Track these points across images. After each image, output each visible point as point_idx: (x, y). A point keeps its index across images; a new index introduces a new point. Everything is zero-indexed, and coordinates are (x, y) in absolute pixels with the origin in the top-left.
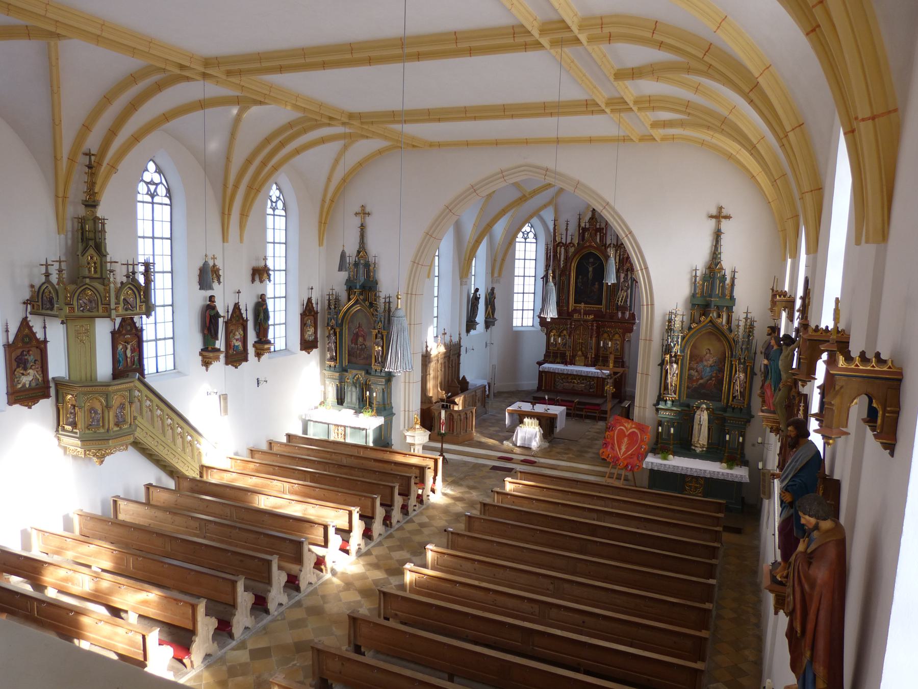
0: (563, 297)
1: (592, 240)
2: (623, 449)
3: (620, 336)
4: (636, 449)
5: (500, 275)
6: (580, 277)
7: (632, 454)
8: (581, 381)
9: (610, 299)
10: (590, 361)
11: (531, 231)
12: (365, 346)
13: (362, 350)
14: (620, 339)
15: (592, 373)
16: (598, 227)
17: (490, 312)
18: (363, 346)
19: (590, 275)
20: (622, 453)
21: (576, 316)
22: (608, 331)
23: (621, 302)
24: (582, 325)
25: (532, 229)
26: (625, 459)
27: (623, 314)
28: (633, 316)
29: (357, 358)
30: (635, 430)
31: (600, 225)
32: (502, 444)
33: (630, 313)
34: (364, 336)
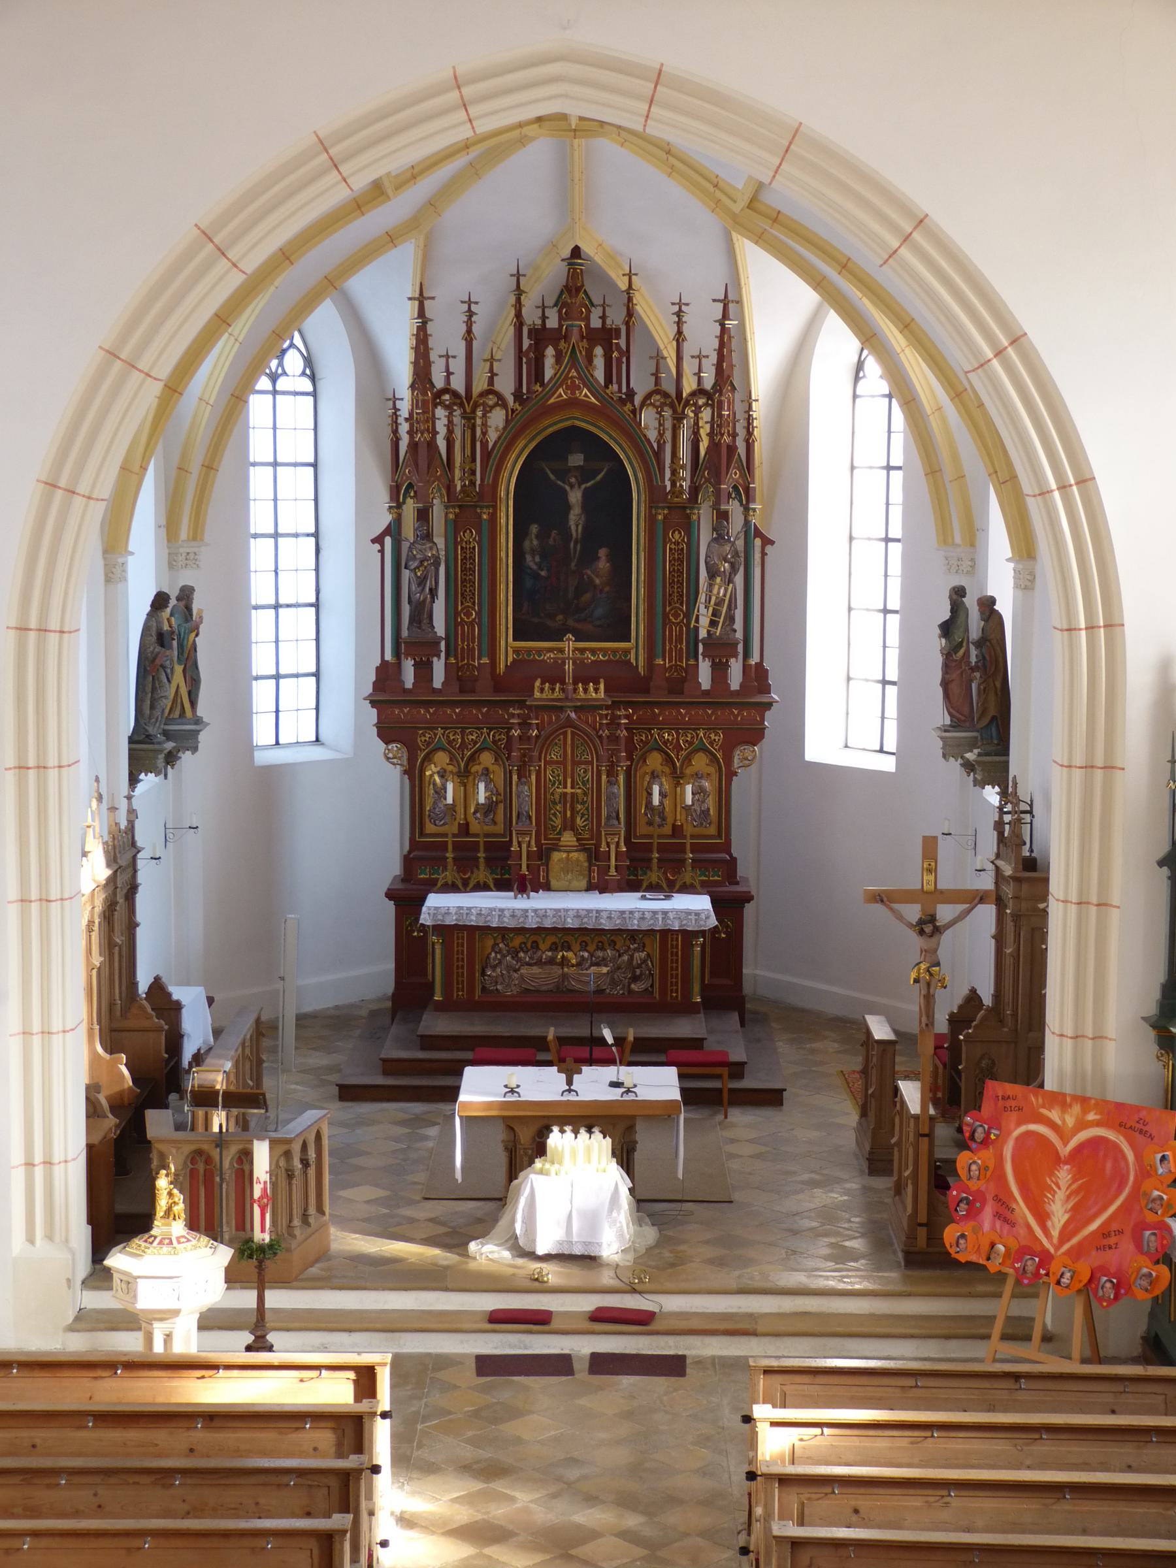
0: (468, 615)
1: (580, 378)
2: (1059, 1214)
3: (714, 759)
4: (1126, 1208)
5: (197, 534)
6: (534, 529)
7: (1104, 1233)
8: (592, 955)
9: (665, 616)
10: (613, 872)
14: (712, 770)
15: (643, 918)
16: (596, 323)
17: (184, 691)
19: (575, 519)
20: (1055, 1233)
21: (541, 693)
22: (666, 743)
23: (713, 623)
24: (569, 723)
26: (1077, 1253)
27: (720, 670)
28: (758, 678)
30: (1111, 1135)
31: (603, 318)
32: (465, 1254)
33: (746, 667)
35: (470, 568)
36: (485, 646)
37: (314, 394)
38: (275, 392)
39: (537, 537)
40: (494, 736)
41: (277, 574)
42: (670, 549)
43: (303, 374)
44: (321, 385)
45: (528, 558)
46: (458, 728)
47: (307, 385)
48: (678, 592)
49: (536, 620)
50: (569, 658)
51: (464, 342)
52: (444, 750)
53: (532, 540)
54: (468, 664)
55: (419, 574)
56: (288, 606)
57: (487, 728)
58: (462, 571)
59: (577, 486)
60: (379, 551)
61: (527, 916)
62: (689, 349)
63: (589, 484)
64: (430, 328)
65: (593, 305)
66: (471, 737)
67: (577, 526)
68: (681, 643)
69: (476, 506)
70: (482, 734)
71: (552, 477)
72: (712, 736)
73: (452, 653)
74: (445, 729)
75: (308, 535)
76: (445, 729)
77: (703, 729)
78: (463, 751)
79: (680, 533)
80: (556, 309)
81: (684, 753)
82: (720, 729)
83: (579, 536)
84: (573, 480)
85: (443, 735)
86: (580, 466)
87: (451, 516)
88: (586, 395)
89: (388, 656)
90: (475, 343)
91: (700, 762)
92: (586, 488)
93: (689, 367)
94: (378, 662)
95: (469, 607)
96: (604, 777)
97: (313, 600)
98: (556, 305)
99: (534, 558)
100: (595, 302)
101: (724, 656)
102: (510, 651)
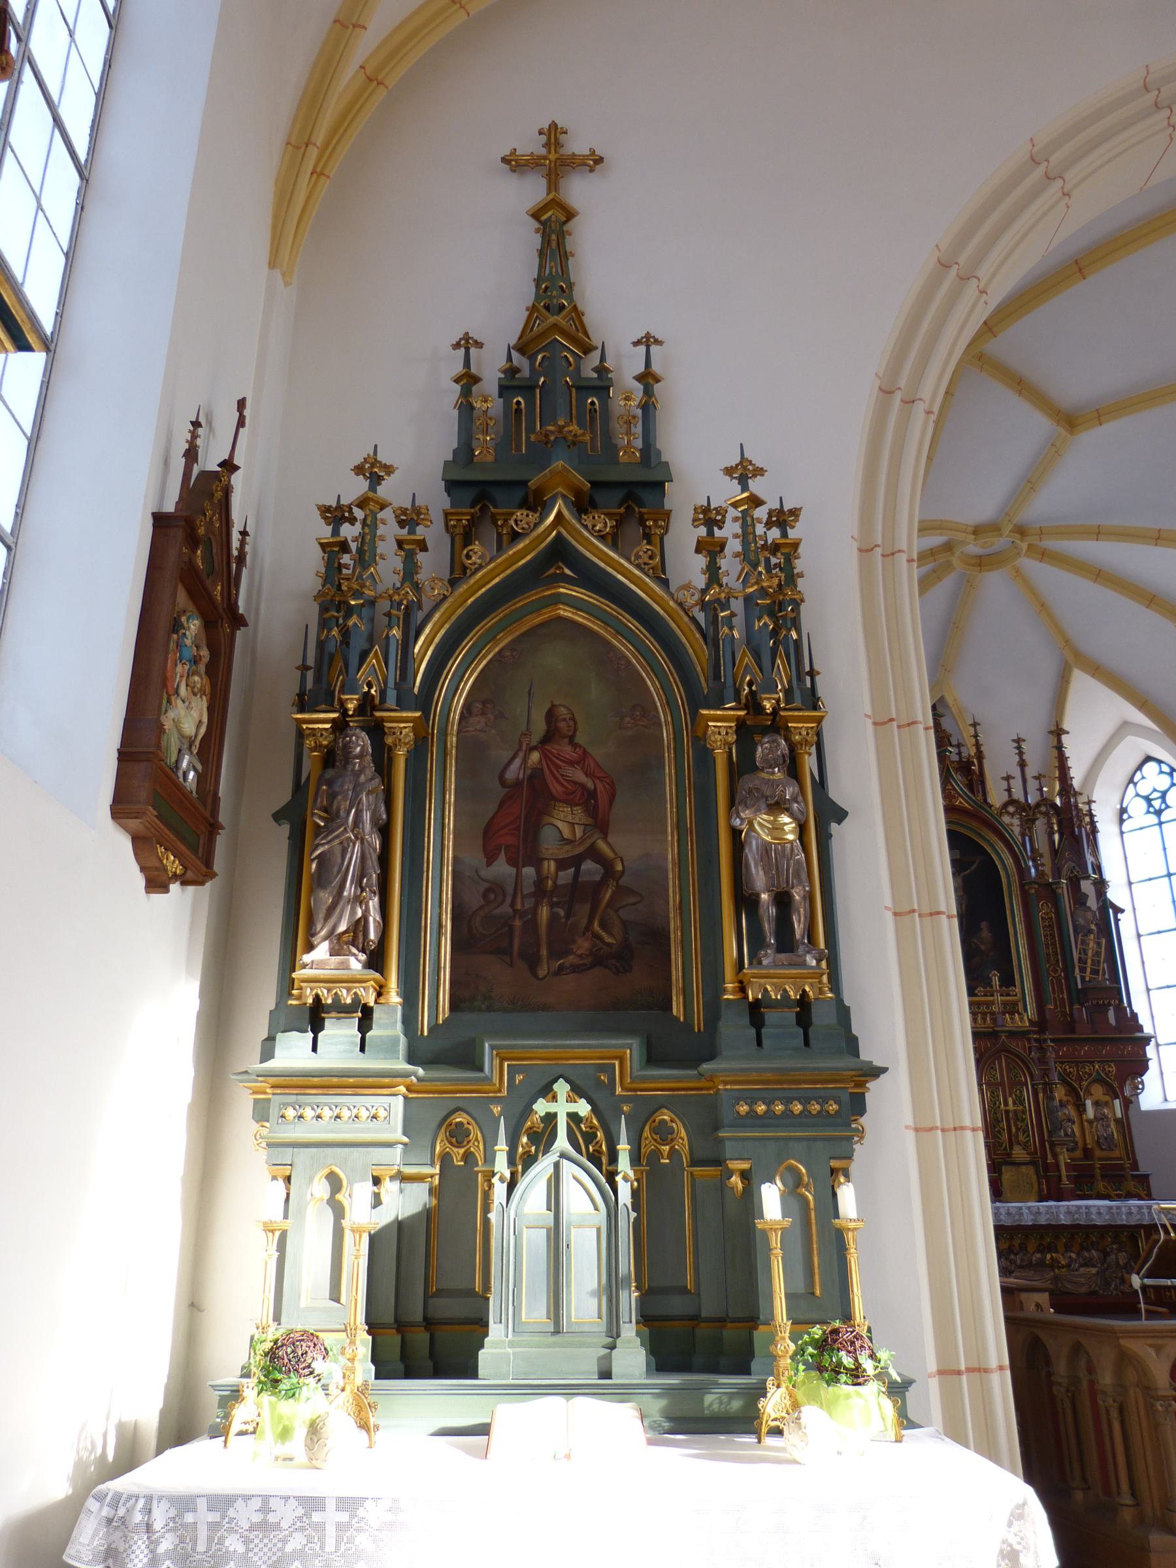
12: (607, 864)
13: (577, 892)
15: (1130, 1213)
18: (588, 865)
29: (533, 963)
34: (593, 794)
42: (1042, 918)
48: (1053, 952)
61: (1022, 1214)
62: (1031, 772)
63: (966, 872)
68: (1063, 994)
72: (1106, 1067)
77: (1098, 1062)
79: (1047, 905)
81: (1085, 1084)
82: (1111, 1061)
88: (960, 803)
91: (1098, 1091)
93: (1032, 785)
96: (1041, 1095)
101: (1106, 999)
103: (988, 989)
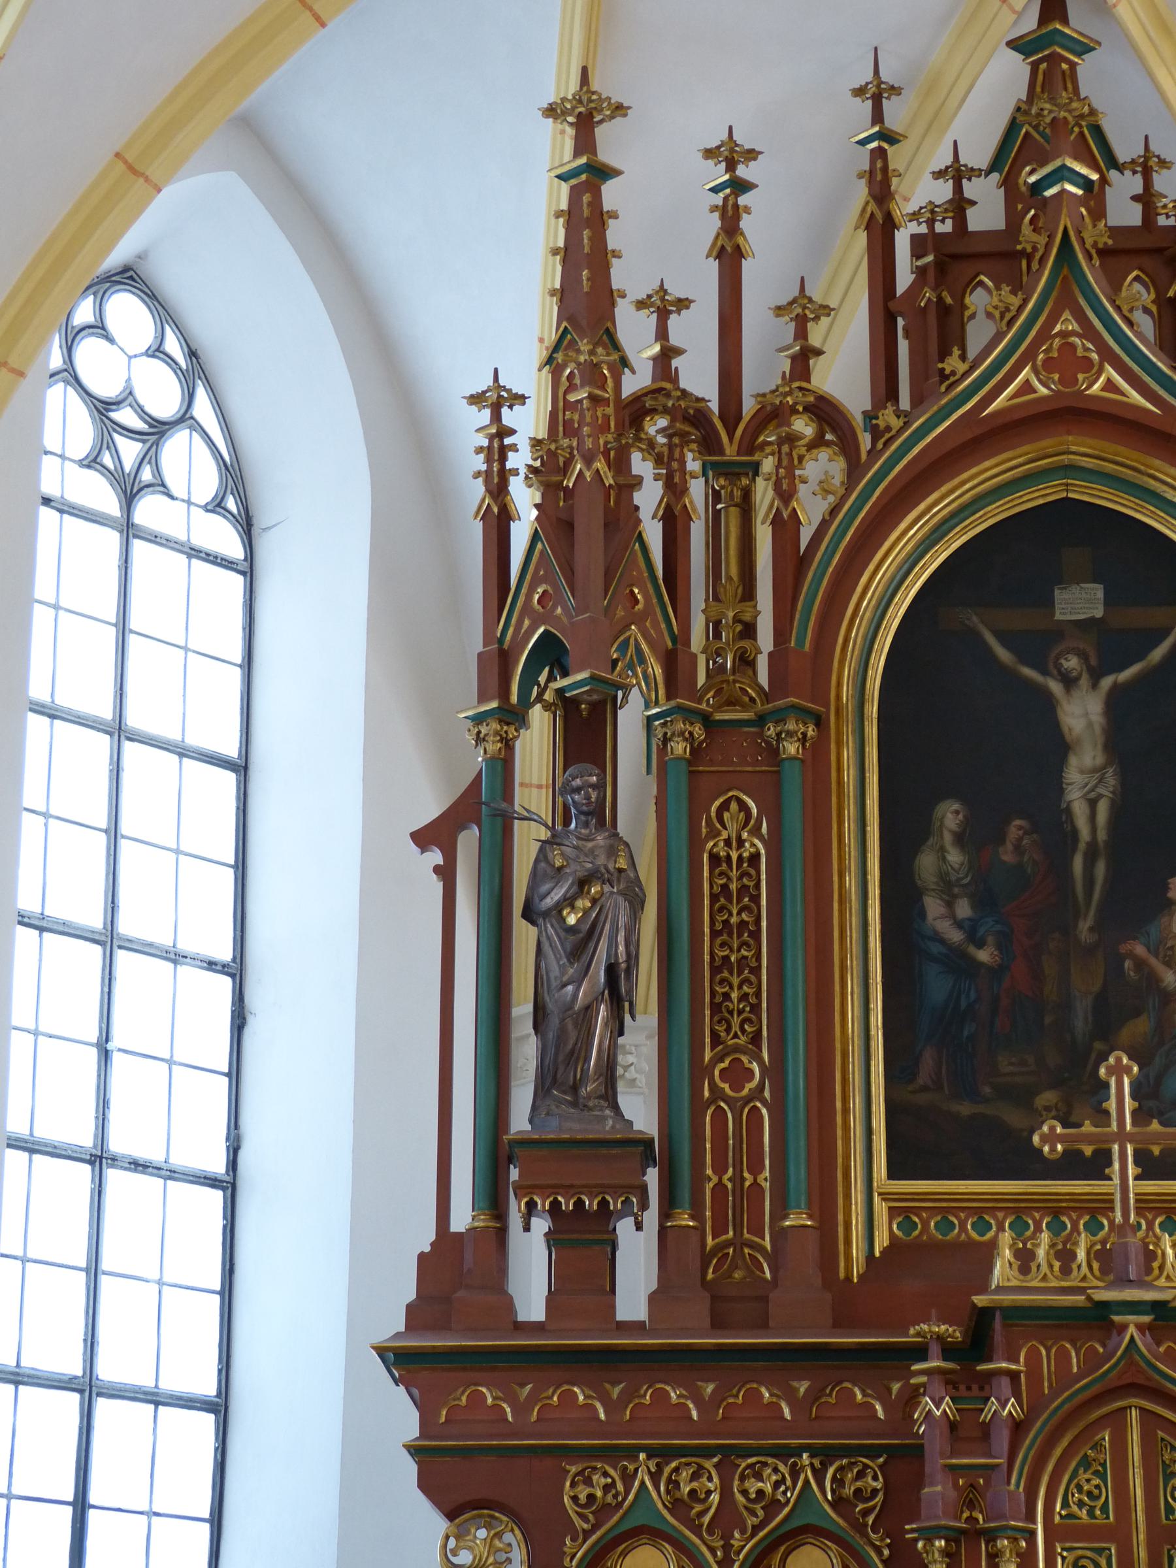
0: (738, 1075)
1: (1089, 332)
11: (185, 418)
25: (201, 393)
31: (1147, 199)
35: (742, 924)
36: (798, 1172)
37: (248, 569)
38: (129, 530)
39: (960, 839)
40: (838, 1481)
41: (105, 1056)
43: (217, 506)
44: (269, 547)
45: (933, 906)
46: (707, 1452)
47: (231, 545)
49: (965, 1109)
50: (1122, 1137)
51: (714, 265)
52: (655, 1534)
53: (942, 850)
54: (739, 1243)
55: (572, 920)
56: (138, 1166)
57: (814, 1452)
58: (714, 934)
59: (1084, 681)
60: (437, 870)
63: (1125, 675)
64: (611, 194)
65: (1112, 162)
66: (753, 1486)
67: (1093, 804)
69: (761, 720)
70: (795, 1474)
71: (1003, 654)
73: (685, 1194)
74: (662, 1454)
75: (211, 965)
76: (662, 1454)
78: (727, 1538)
80: (995, 177)
83: (1102, 835)
84: (1072, 663)
85: (655, 1477)
86: (1092, 620)
87: (679, 748)
88: (1110, 386)
89: (462, 1218)
90: (748, 267)
92: (1115, 686)
94: (425, 1239)
95: (737, 1049)
97: (218, 1165)
98: (994, 166)
99: (950, 905)
100: (1123, 154)
102: (881, 1208)
103: (1088, 1127)
